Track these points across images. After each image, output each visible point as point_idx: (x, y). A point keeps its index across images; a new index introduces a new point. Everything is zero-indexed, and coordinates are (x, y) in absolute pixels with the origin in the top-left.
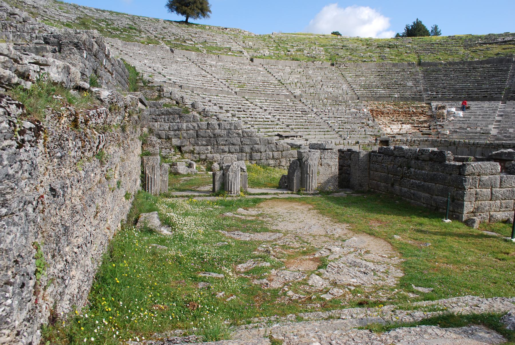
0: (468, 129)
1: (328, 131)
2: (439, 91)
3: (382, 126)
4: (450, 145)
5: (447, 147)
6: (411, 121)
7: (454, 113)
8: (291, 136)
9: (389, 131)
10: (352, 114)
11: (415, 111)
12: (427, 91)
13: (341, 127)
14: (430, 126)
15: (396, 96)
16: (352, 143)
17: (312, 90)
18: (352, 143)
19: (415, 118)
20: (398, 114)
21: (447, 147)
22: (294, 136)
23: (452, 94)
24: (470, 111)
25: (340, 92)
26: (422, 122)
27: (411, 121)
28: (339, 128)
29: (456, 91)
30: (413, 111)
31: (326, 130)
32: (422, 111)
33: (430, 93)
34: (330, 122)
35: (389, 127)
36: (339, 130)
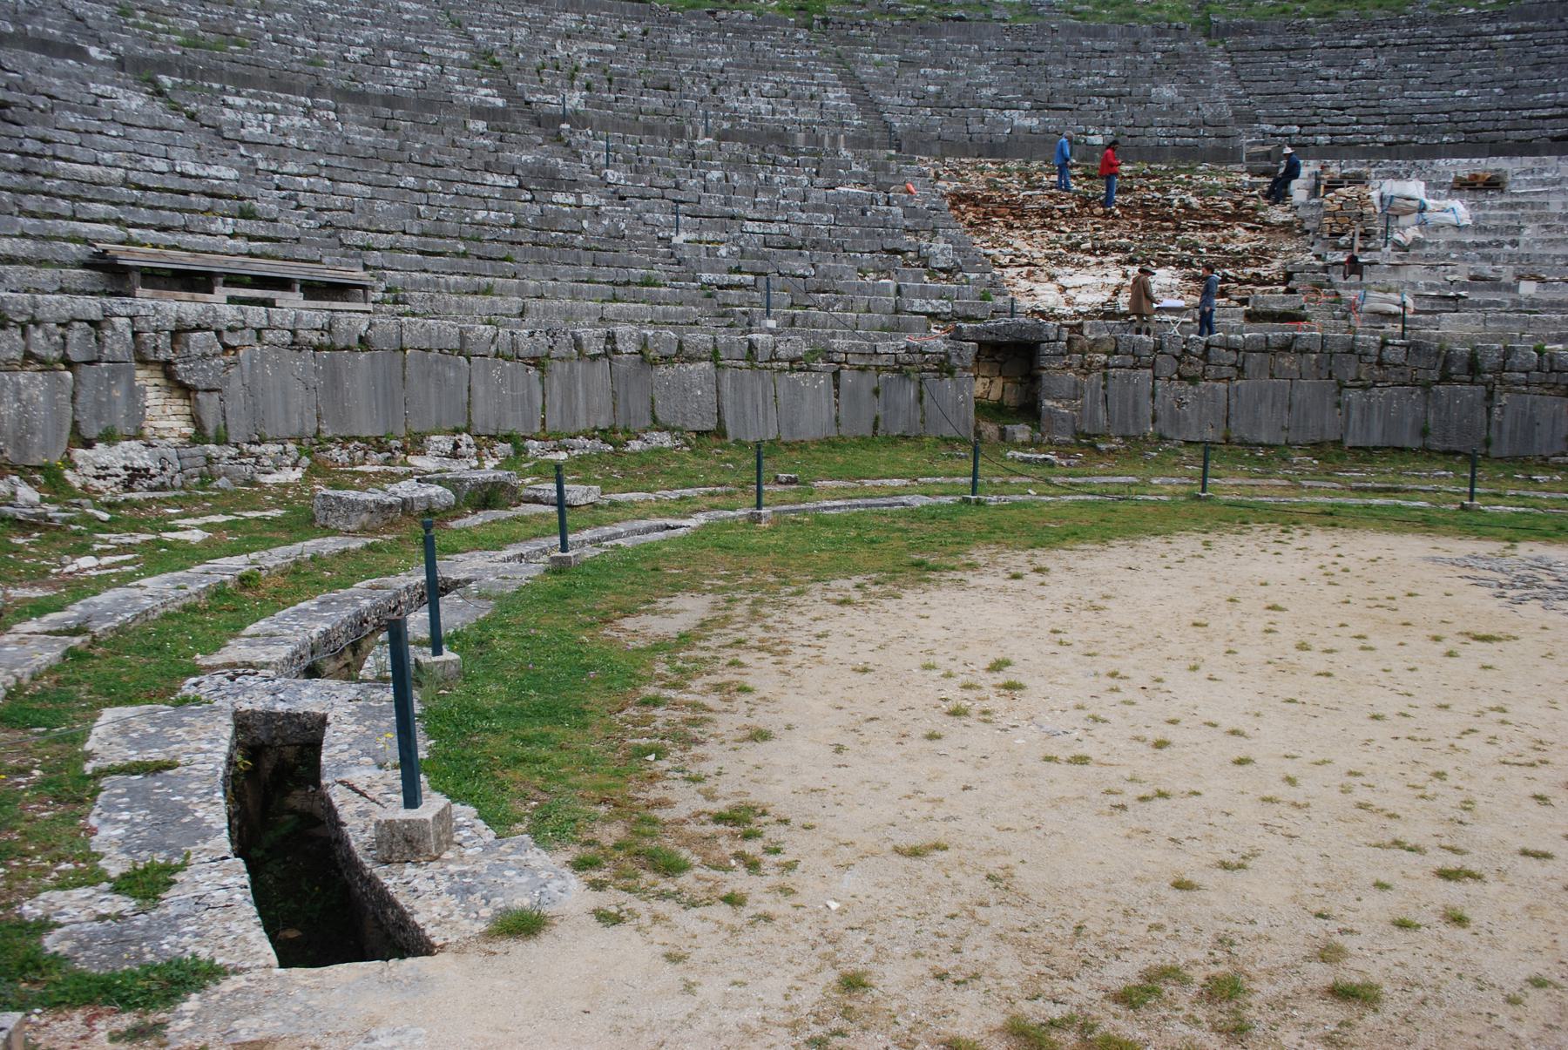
0: (1528, 288)
1: (648, 282)
2: (1315, 120)
3: (1012, 272)
4: (1446, 378)
5: (1426, 387)
6: (1175, 250)
7: (1423, 209)
8: (233, 280)
9: (1048, 296)
10: (838, 207)
11: (1195, 202)
12: (1256, 119)
13: (745, 264)
14: (1289, 276)
15: (1098, 140)
16: (783, 350)
17: (655, 101)
18: (783, 350)
19: (1200, 237)
20: (1105, 215)
21: (1426, 387)
22: (284, 284)
23: (1382, 132)
24: (1507, 200)
25: (806, 114)
26: (1239, 260)
27: (1175, 250)
28: (738, 270)
29: (1402, 121)
30: (1187, 206)
31: (637, 272)
32: (1238, 204)
33: (1268, 127)
34: (683, 236)
35: (1052, 278)
36: (728, 278)
